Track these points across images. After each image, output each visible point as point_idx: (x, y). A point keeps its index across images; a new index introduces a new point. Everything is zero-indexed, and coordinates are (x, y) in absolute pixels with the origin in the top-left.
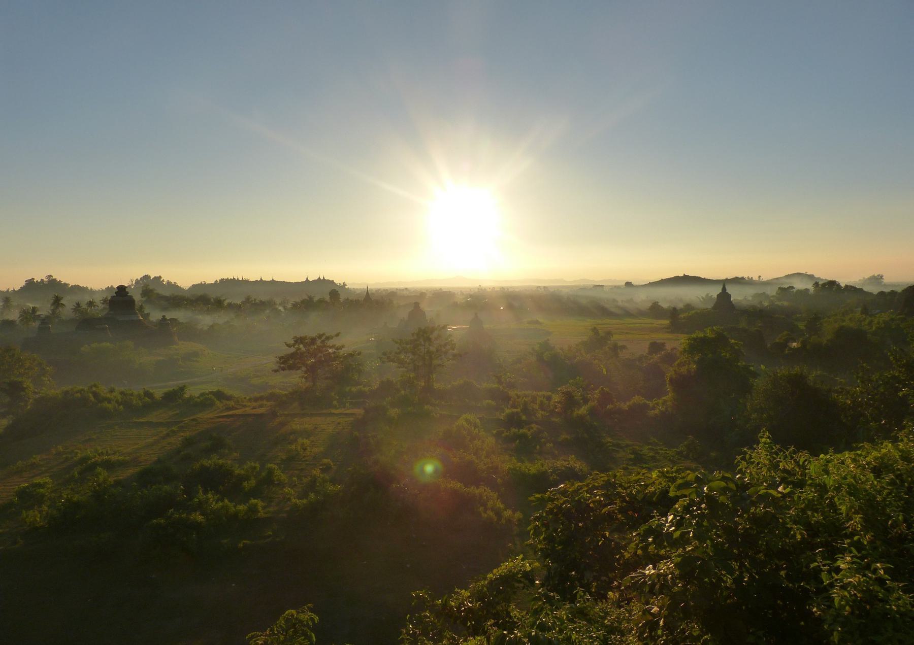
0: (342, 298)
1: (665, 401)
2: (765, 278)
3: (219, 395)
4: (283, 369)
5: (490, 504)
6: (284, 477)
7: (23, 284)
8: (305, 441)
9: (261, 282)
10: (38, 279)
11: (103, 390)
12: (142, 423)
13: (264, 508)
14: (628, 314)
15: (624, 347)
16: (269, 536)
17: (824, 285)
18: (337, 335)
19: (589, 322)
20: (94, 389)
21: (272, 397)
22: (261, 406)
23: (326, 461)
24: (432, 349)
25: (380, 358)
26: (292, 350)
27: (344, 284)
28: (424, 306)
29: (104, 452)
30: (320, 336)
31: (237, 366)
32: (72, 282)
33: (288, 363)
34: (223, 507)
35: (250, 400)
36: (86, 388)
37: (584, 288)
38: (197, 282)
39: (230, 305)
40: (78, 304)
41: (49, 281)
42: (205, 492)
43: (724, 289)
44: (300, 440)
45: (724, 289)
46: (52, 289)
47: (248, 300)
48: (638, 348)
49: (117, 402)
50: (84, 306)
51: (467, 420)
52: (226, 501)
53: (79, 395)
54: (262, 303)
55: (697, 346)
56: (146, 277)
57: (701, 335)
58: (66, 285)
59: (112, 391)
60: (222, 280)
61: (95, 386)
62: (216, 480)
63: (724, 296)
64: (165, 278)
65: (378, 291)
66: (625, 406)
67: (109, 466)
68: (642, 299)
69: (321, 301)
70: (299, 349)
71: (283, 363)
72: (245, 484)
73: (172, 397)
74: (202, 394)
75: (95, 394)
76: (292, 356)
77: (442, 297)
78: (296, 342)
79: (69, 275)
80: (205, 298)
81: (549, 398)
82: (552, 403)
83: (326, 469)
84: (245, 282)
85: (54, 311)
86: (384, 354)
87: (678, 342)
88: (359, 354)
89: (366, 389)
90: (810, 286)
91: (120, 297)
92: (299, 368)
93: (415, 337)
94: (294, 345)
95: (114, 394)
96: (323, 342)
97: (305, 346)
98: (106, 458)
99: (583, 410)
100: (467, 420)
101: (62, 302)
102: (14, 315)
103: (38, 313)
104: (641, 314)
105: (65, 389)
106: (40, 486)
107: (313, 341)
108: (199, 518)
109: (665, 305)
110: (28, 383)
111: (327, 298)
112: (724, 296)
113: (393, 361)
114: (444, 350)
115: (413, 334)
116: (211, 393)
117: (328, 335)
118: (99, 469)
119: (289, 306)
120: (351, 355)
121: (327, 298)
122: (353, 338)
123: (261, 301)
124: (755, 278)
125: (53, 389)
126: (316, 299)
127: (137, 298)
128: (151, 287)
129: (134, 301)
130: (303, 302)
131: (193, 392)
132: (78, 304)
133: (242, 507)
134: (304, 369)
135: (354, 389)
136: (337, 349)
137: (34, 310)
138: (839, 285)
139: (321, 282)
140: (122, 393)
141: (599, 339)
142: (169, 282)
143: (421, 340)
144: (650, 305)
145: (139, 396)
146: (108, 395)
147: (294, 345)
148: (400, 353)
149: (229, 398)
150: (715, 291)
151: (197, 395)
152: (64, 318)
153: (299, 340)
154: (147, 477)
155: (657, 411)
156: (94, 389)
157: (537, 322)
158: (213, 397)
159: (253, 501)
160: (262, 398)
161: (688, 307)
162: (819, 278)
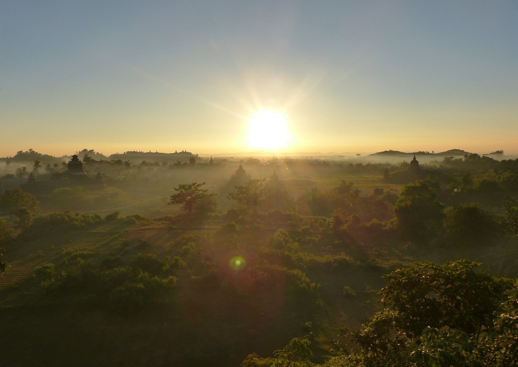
1: (392, 222)
2: (436, 152)
3: (138, 217)
4: (173, 203)
7: (16, 154)
11: (72, 214)
18: (204, 184)
20: (68, 214)
21: (167, 219)
25: (228, 197)
26: (179, 192)
28: (247, 169)
30: (194, 184)
31: (148, 200)
32: (43, 153)
33: (176, 199)
35: (154, 220)
43: (415, 158)
45: (415, 158)
46: (32, 157)
49: (81, 220)
53: (59, 217)
55: (409, 191)
57: (412, 185)
59: (77, 215)
60: (128, 152)
61: (68, 212)
63: (415, 162)
64: (96, 151)
66: (368, 225)
70: (182, 192)
71: (173, 199)
73: (111, 218)
74: (128, 217)
75: (69, 217)
77: (253, 162)
78: (180, 187)
80: (120, 161)
81: (325, 220)
82: (327, 223)
85: (35, 169)
87: (399, 189)
92: (182, 202)
94: (179, 190)
96: (195, 188)
99: (345, 227)
103: (26, 171)
107: (190, 186)
111: (188, 162)
112: (415, 162)
113: (235, 198)
115: (246, 184)
116: (133, 216)
117: (198, 183)
120: (212, 195)
124: (431, 152)
125: (45, 214)
128: (89, 156)
131: (123, 215)
135: (213, 214)
136: (204, 191)
137: (24, 168)
138: (479, 157)
140: (83, 216)
142: (98, 153)
145: (92, 217)
146: (76, 217)
147: (179, 190)
148: (240, 194)
149: (143, 219)
150: (409, 160)
153: (182, 187)
156: (68, 214)
158: (134, 219)
161: (394, 168)
162: (467, 152)
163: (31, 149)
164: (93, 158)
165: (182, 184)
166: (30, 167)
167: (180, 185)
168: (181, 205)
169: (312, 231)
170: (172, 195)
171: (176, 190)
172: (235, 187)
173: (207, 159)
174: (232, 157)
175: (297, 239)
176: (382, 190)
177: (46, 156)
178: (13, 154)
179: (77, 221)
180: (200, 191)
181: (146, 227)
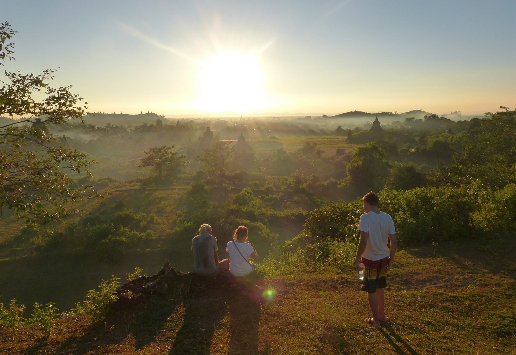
0: (164, 123)
1: (346, 181)
4: (144, 166)
5: (264, 230)
6: (159, 220)
9: (114, 115)
13: (154, 234)
14: (324, 132)
15: (323, 152)
16: (159, 247)
17: (430, 117)
18: (173, 147)
19: (303, 138)
21: (139, 181)
22: (134, 186)
23: (178, 212)
26: (149, 155)
27: (163, 116)
30: (163, 148)
33: (146, 162)
34: (134, 234)
35: (126, 182)
37: (300, 118)
39: (98, 128)
47: (108, 125)
48: (330, 152)
51: (246, 191)
52: (135, 231)
54: (117, 127)
62: (126, 221)
65: (183, 119)
66: (326, 183)
68: (333, 125)
69: (151, 126)
72: (141, 223)
74: (100, 180)
76: (149, 159)
78: (150, 151)
81: (287, 180)
82: (288, 182)
83: (179, 216)
84: (105, 115)
86: (198, 157)
87: (353, 149)
89: (189, 176)
90: (422, 117)
94: (149, 153)
99: (304, 186)
100: (246, 191)
104: (333, 133)
107: (160, 150)
109: (345, 128)
113: (203, 161)
115: (214, 146)
117: (168, 147)
119: (133, 129)
120: (181, 158)
121: (155, 124)
122: (178, 147)
123: (116, 126)
126: (148, 125)
130: (141, 126)
131: (95, 178)
133: (144, 234)
136: (173, 154)
141: (309, 148)
144: (336, 128)
148: (207, 156)
153: (153, 150)
154: (88, 221)
155: (342, 186)
157: (275, 138)
159: (148, 231)
168: (151, 168)
169: (275, 190)
170: (142, 158)
173: (174, 120)
175: (260, 197)
176: (344, 150)
181: (119, 189)
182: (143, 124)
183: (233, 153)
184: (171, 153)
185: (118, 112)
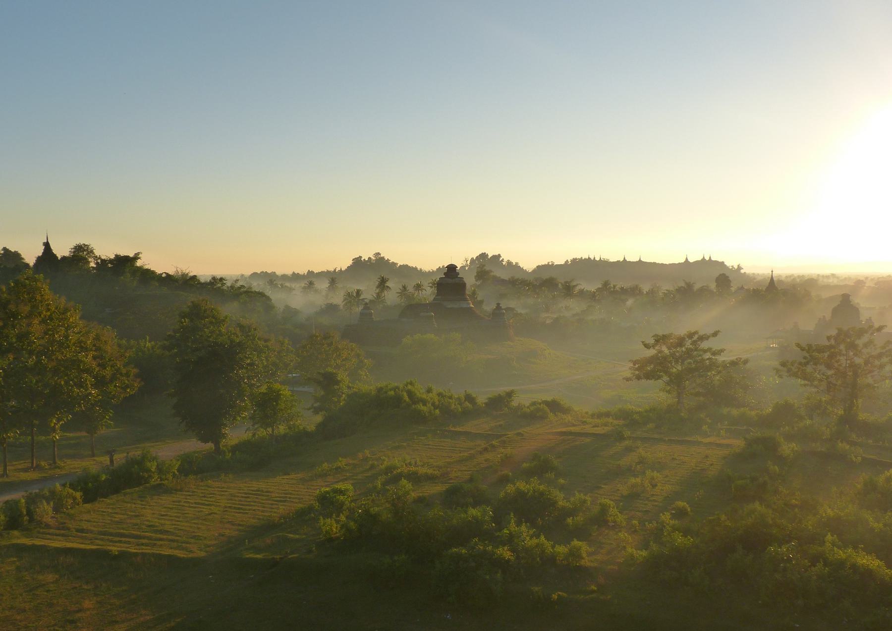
3: (554, 406)
4: (638, 378)
6: (621, 518)
7: (349, 263)
8: (655, 474)
9: (624, 264)
10: (365, 257)
11: (420, 391)
12: (461, 433)
13: (590, 554)
16: (593, 592)
18: (715, 334)
23: (681, 504)
24: (858, 361)
26: (651, 352)
27: (739, 268)
29: (413, 462)
30: (691, 335)
32: (400, 262)
34: (537, 545)
35: (593, 416)
36: (401, 386)
38: (544, 262)
39: (582, 292)
40: (404, 287)
41: (376, 260)
42: (519, 524)
44: (649, 473)
46: (376, 269)
49: (433, 404)
50: (410, 289)
52: (542, 538)
53: (392, 393)
56: (483, 256)
58: (394, 264)
59: (429, 391)
60: (574, 260)
61: (411, 383)
62: (532, 509)
64: (505, 257)
67: (415, 479)
69: (704, 290)
70: (660, 352)
71: (637, 369)
72: (570, 520)
73: (498, 403)
74: (534, 404)
75: (410, 393)
78: (657, 341)
79: (399, 254)
80: (552, 282)
83: (680, 514)
84: (603, 265)
85: (378, 295)
88: (746, 362)
91: (450, 280)
92: (659, 377)
93: (833, 342)
95: (430, 395)
96: (694, 343)
97: (669, 348)
98: (413, 469)
101: (388, 284)
102: (338, 299)
105: (379, 385)
106: (341, 492)
107: (681, 342)
108: (505, 553)
110: (342, 376)
111: (713, 286)
114: (877, 363)
115: (829, 338)
116: (546, 403)
117: (701, 333)
118: (404, 482)
120: (734, 363)
123: (622, 288)
125: (368, 384)
126: (697, 287)
127: (470, 281)
128: (487, 268)
129: (464, 285)
130: (679, 290)
131: (523, 400)
132: (404, 287)
133: (561, 549)
134: (666, 378)
135: (735, 412)
136: (714, 354)
139: (706, 264)
140: (439, 394)
142: (509, 263)
143: (842, 347)
145: (459, 399)
146: (424, 396)
147: (654, 346)
148: (806, 364)
151: (527, 404)
152: (389, 303)
153: (660, 339)
154: (454, 497)
156: (410, 387)
158: (546, 408)
159: (576, 543)
160: (607, 415)
163: (379, 254)
164: (498, 273)
165: (661, 333)
166: (368, 288)
167: (656, 335)
171: (647, 346)
172: (798, 345)
174: (833, 275)
177: (406, 267)
178: (344, 263)
179: (425, 405)
180: (705, 351)
182: (683, 285)
183: (885, 360)
184: (709, 350)
185: (632, 258)
